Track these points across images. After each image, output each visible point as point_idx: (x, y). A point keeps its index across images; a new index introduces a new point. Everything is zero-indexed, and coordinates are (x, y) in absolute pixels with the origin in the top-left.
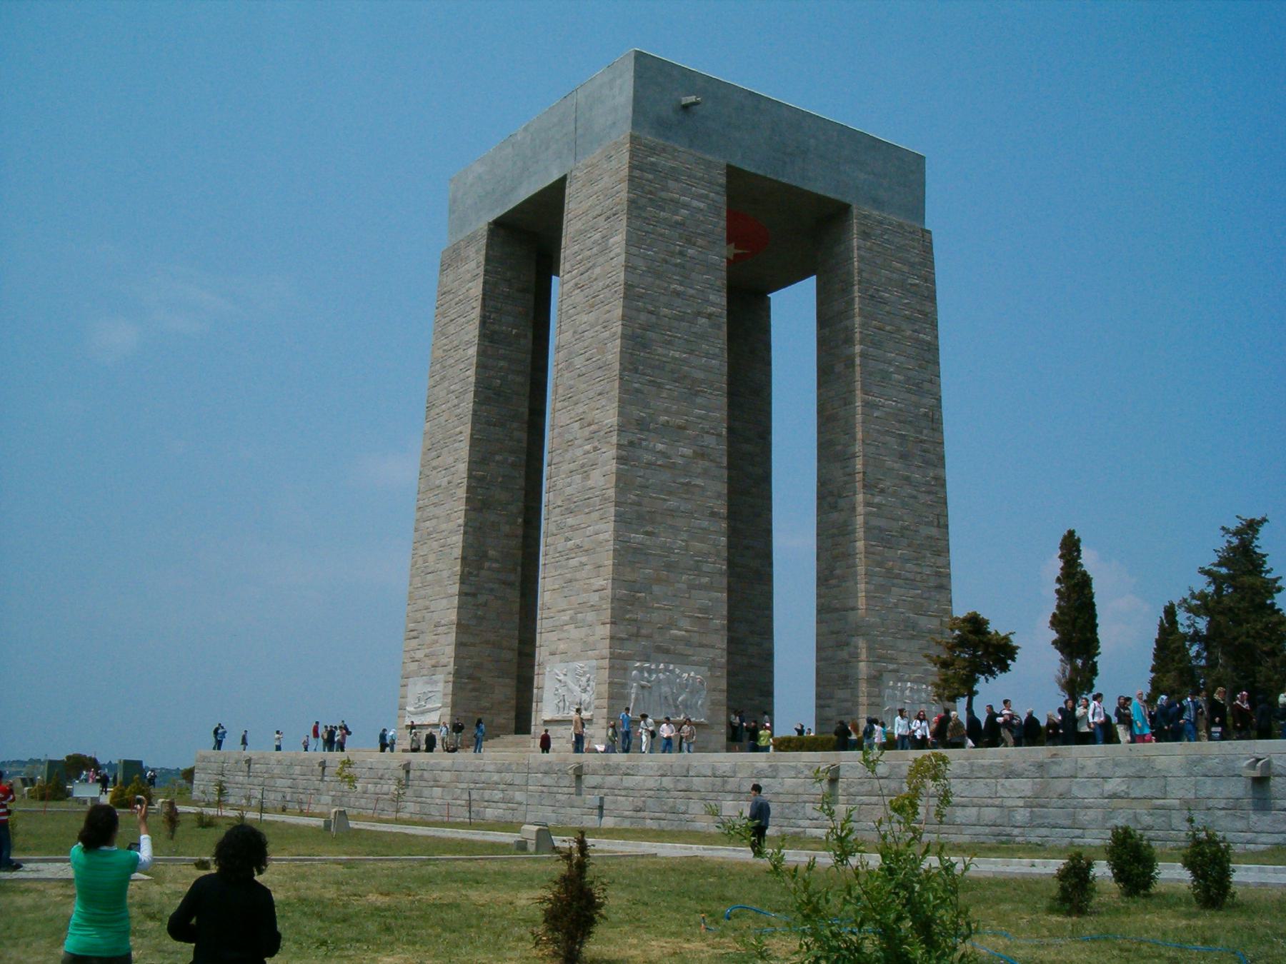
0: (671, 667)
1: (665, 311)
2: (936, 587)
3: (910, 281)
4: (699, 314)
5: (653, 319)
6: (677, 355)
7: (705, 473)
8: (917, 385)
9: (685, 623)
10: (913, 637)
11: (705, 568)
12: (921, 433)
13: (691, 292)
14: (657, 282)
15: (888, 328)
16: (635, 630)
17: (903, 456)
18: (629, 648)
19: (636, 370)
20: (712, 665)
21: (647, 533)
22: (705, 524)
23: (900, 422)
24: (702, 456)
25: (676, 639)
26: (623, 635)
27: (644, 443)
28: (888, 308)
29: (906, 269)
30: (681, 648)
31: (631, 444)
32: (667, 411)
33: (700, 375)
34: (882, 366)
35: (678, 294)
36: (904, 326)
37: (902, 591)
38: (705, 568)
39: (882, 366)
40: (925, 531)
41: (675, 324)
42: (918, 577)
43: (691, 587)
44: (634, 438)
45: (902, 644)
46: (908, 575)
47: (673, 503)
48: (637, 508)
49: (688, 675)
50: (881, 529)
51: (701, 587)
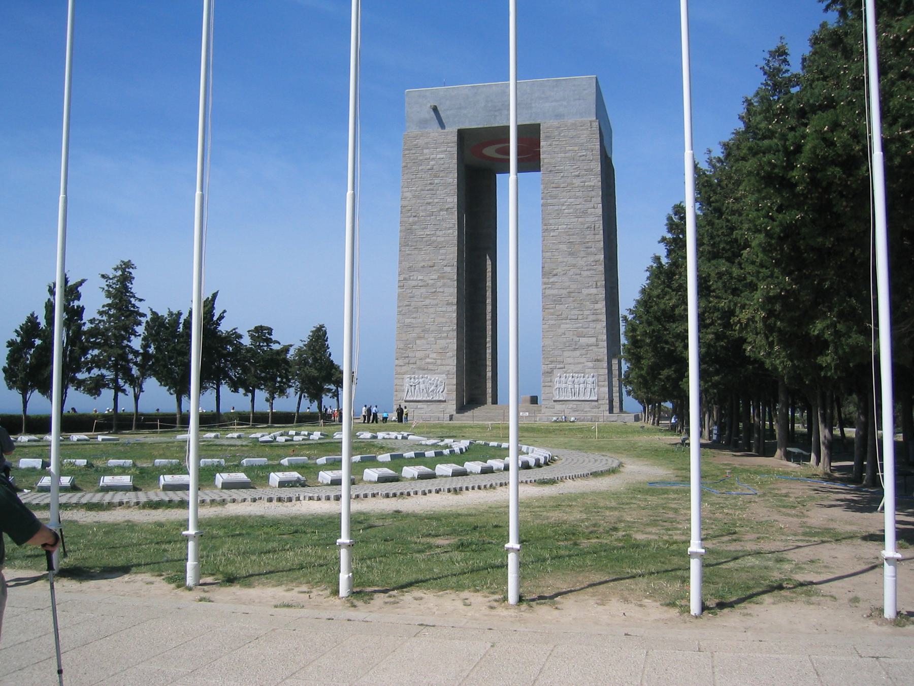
0: (426, 376)
1: (421, 214)
2: (594, 321)
3: (580, 154)
4: (441, 210)
5: (416, 219)
6: (429, 233)
7: (444, 285)
8: (583, 212)
9: (434, 356)
10: (575, 349)
11: (444, 329)
12: (585, 238)
13: (436, 200)
14: (419, 201)
15: (562, 185)
16: (407, 361)
17: (571, 254)
18: (404, 369)
19: (408, 245)
20: (448, 373)
21: (413, 318)
22: (444, 309)
23: (569, 235)
24: (443, 277)
25: (428, 363)
26: (402, 364)
27: (411, 278)
28: (562, 174)
29: (576, 148)
30: (430, 367)
31: (405, 279)
32: (423, 260)
33: (443, 239)
34: (556, 208)
35: (429, 204)
36: (574, 181)
37: (568, 326)
38: (444, 329)
39: (556, 208)
40: (585, 291)
41: (429, 218)
42: (580, 317)
43: (436, 339)
44: (407, 276)
45: (566, 354)
46: (573, 317)
47: (427, 302)
48: (407, 307)
49: (439, 378)
50: (554, 295)
51: (441, 338)
